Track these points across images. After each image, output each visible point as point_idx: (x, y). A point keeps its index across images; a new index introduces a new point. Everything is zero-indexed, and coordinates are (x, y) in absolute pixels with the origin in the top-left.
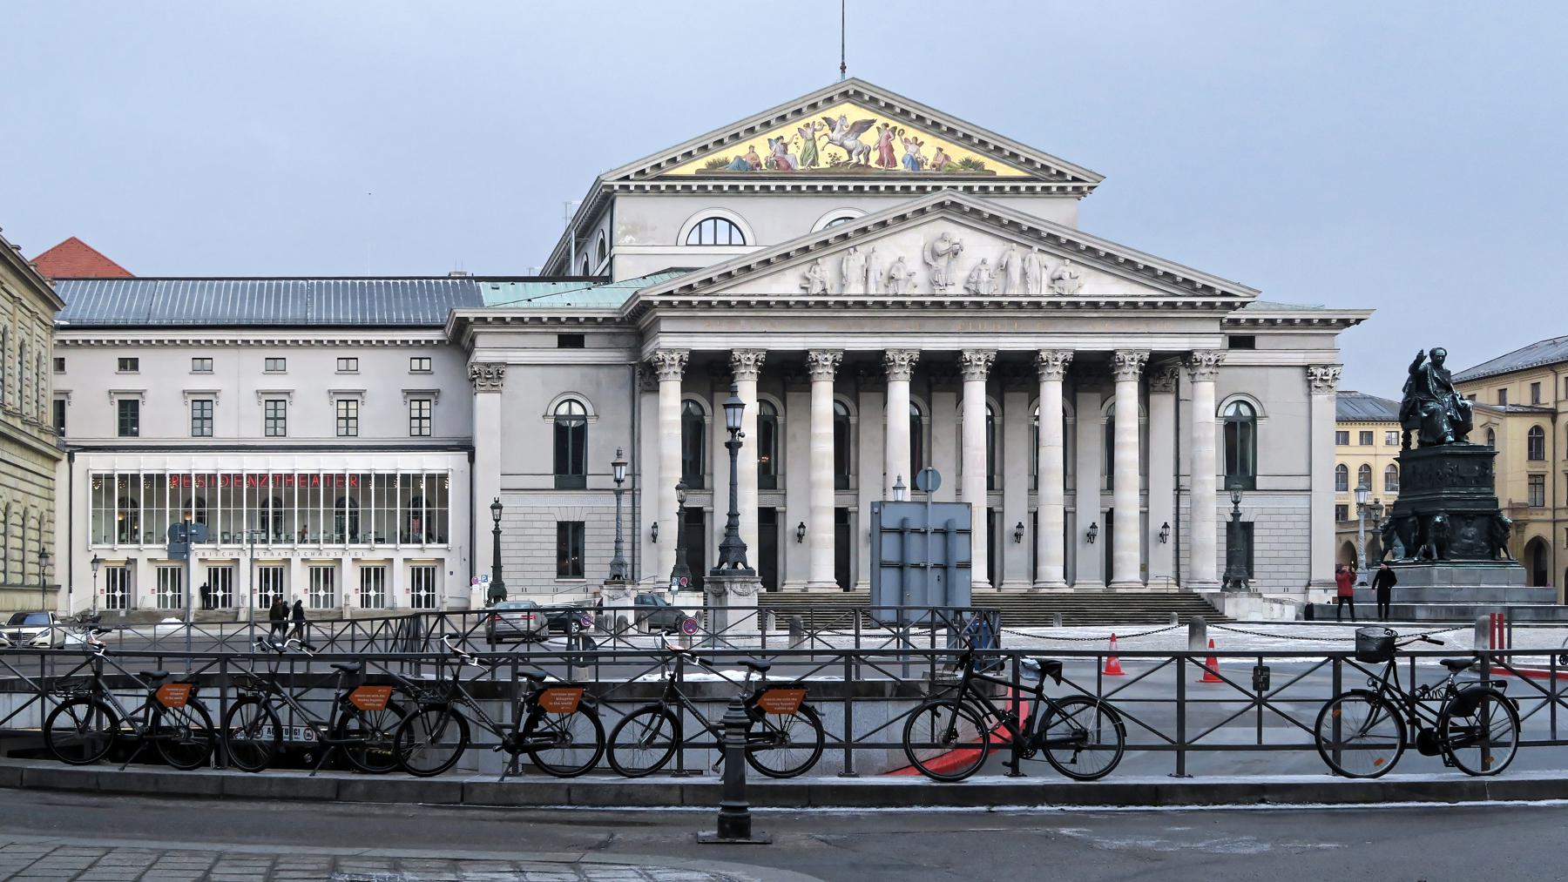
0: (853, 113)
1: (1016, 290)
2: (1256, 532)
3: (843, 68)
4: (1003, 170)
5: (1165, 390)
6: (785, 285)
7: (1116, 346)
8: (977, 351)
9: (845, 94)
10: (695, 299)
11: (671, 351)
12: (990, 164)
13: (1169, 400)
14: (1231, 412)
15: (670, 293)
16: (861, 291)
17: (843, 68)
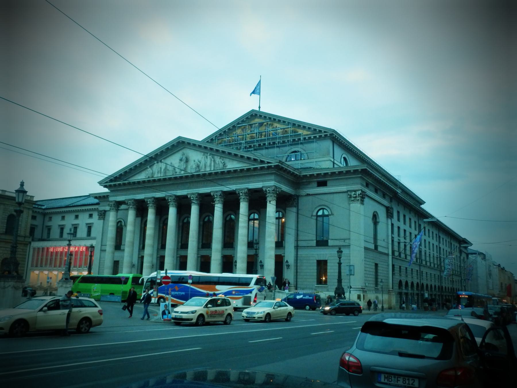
0: (257, 120)
1: (202, 171)
2: (328, 264)
3: (259, 107)
4: (305, 132)
5: (292, 206)
6: (142, 177)
7: (237, 188)
8: (193, 194)
9: (252, 115)
10: (112, 184)
11: (111, 202)
12: (300, 132)
13: (294, 209)
14: (320, 213)
15: (107, 182)
16: (159, 175)
17: (259, 107)
